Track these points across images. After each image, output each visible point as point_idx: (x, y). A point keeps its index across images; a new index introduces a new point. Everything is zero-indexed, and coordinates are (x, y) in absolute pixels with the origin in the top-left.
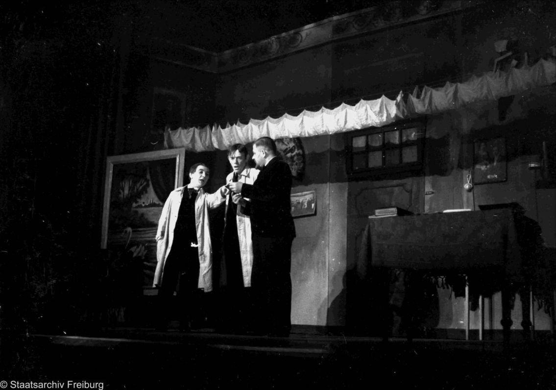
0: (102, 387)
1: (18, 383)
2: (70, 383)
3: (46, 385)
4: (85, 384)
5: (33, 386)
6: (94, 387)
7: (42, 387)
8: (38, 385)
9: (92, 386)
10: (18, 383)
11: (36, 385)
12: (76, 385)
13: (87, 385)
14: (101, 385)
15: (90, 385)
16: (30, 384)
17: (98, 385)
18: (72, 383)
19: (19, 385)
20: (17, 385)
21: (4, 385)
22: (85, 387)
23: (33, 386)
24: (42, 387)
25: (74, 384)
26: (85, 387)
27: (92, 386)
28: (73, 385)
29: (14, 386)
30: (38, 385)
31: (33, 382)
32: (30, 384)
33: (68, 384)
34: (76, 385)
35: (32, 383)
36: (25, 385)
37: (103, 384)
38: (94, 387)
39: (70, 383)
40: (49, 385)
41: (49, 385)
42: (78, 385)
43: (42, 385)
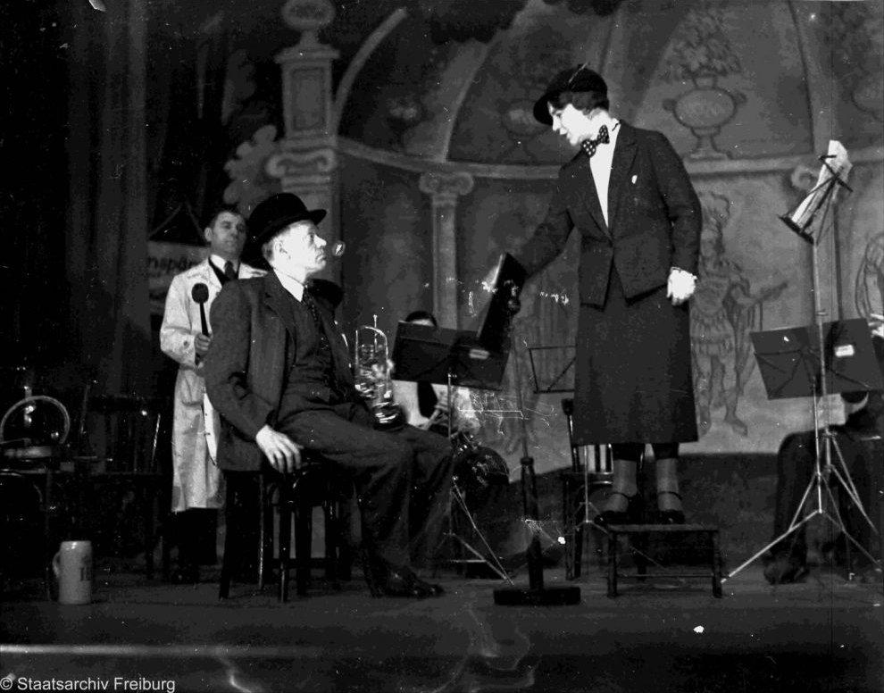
0: (173, 688)
1: (30, 681)
2: (118, 681)
3: (78, 684)
4: (144, 683)
5: (56, 686)
7: (71, 688)
9: (156, 686)
10: (30, 681)
12: (128, 684)
13: (147, 685)
15: (152, 685)
17: (165, 685)
18: (123, 681)
19: (33, 685)
22: (144, 688)
23: (56, 686)
24: (71, 688)
25: (126, 683)
27: (156, 686)
28: (123, 683)
29: (23, 686)
31: (56, 680)
33: (116, 684)
34: (128, 684)
35: (53, 681)
36: (42, 685)
37: (173, 682)
39: (118, 681)
41: (84, 685)
42: (133, 685)
43: (71, 685)
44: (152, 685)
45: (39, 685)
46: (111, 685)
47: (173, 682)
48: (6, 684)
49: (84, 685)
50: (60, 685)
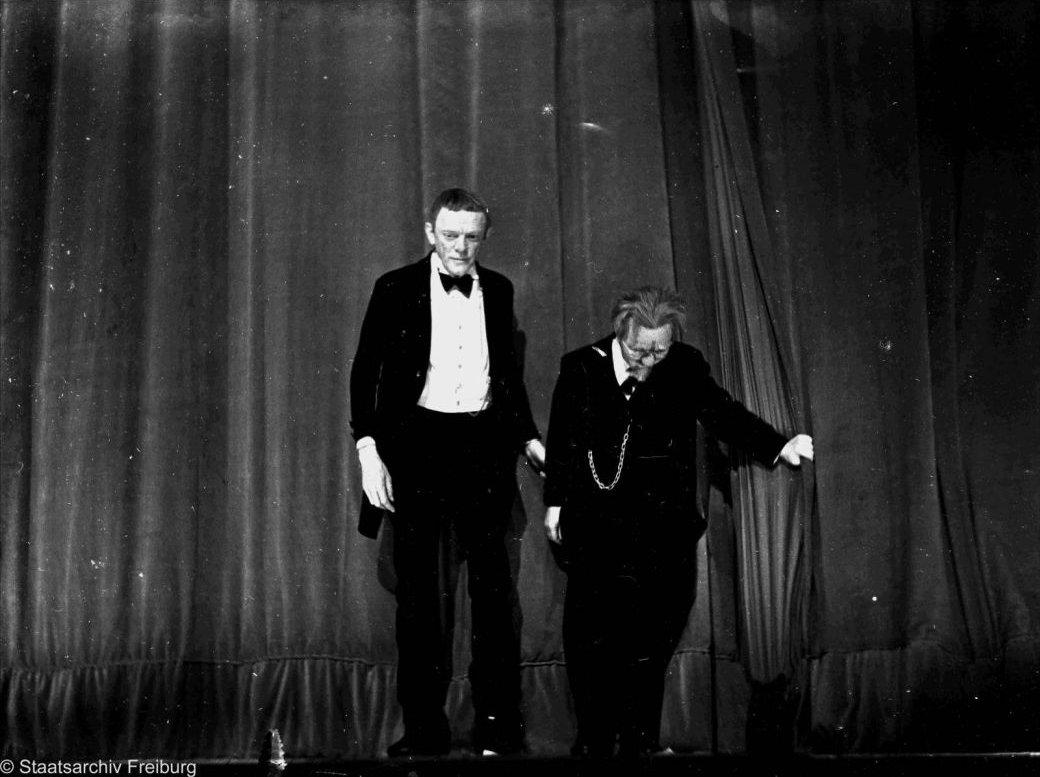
0: (194, 772)
1: (34, 764)
2: (132, 764)
3: (87, 767)
5: (63, 769)
6: (178, 771)
8: (72, 768)
9: (175, 769)
10: (34, 764)
11: (67, 768)
12: (144, 767)
13: (165, 768)
14: (191, 768)
15: (170, 768)
16: (58, 767)
17: (185, 767)
19: (37, 768)
20: (31, 766)
21: (7, 767)
22: (162, 771)
23: (63, 769)
26: (162, 771)
27: (175, 769)
28: (138, 766)
29: (26, 770)
30: (72, 768)
32: (58, 767)
34: (144, 767)
35: (60, 764)
36: (47, 768)
38: (178, 771)
40: (94, 768)
42: (148, 767)
44: (170, 768)
45: (43, 769)
46: (125, 767)
47: (194, 765)
48: (7, 767)
49: (94, 768)
50: (67, 768)
